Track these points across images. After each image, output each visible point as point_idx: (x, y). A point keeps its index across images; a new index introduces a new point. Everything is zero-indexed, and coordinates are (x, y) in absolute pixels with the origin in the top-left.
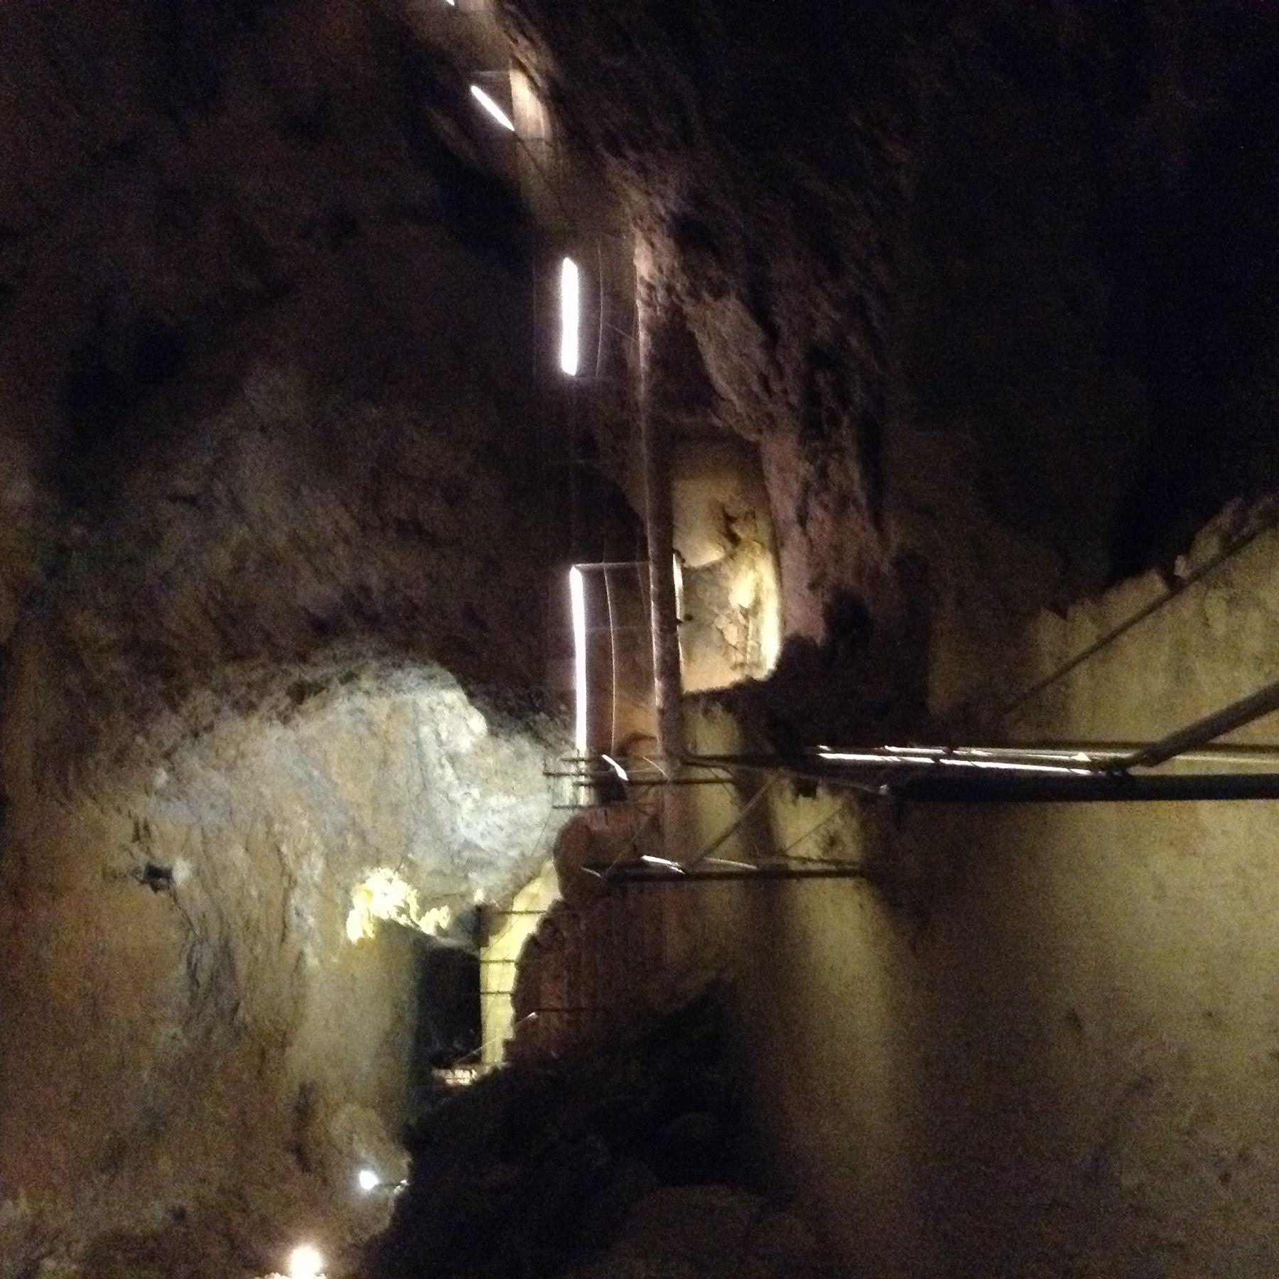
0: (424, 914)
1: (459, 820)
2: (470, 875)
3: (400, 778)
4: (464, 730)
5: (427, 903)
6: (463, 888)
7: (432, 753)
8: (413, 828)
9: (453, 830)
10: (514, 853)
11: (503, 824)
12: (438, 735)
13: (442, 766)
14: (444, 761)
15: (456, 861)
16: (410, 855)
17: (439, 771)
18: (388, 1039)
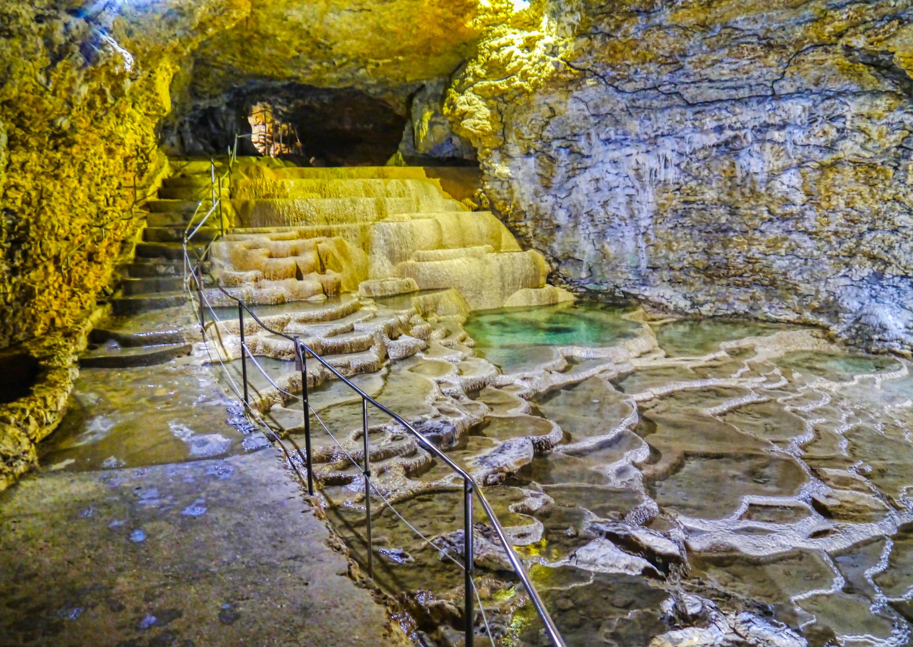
0: (485, 99)
1: (628, 151)
2: (531, 161)
3: (725, 71)
4: (780, 164)
5: (504, 105)
6: (515, 151)
7: (748, 116)
8: (629, 87)
9: (608, 141)
10: (562, 217)
11: (611, 210)
12: (782, 126)
13: (720, 129)
14: (729, 133)
15: (556, 144)
16: (590, 82)
17: (710, 123)
18: (320, 48)
